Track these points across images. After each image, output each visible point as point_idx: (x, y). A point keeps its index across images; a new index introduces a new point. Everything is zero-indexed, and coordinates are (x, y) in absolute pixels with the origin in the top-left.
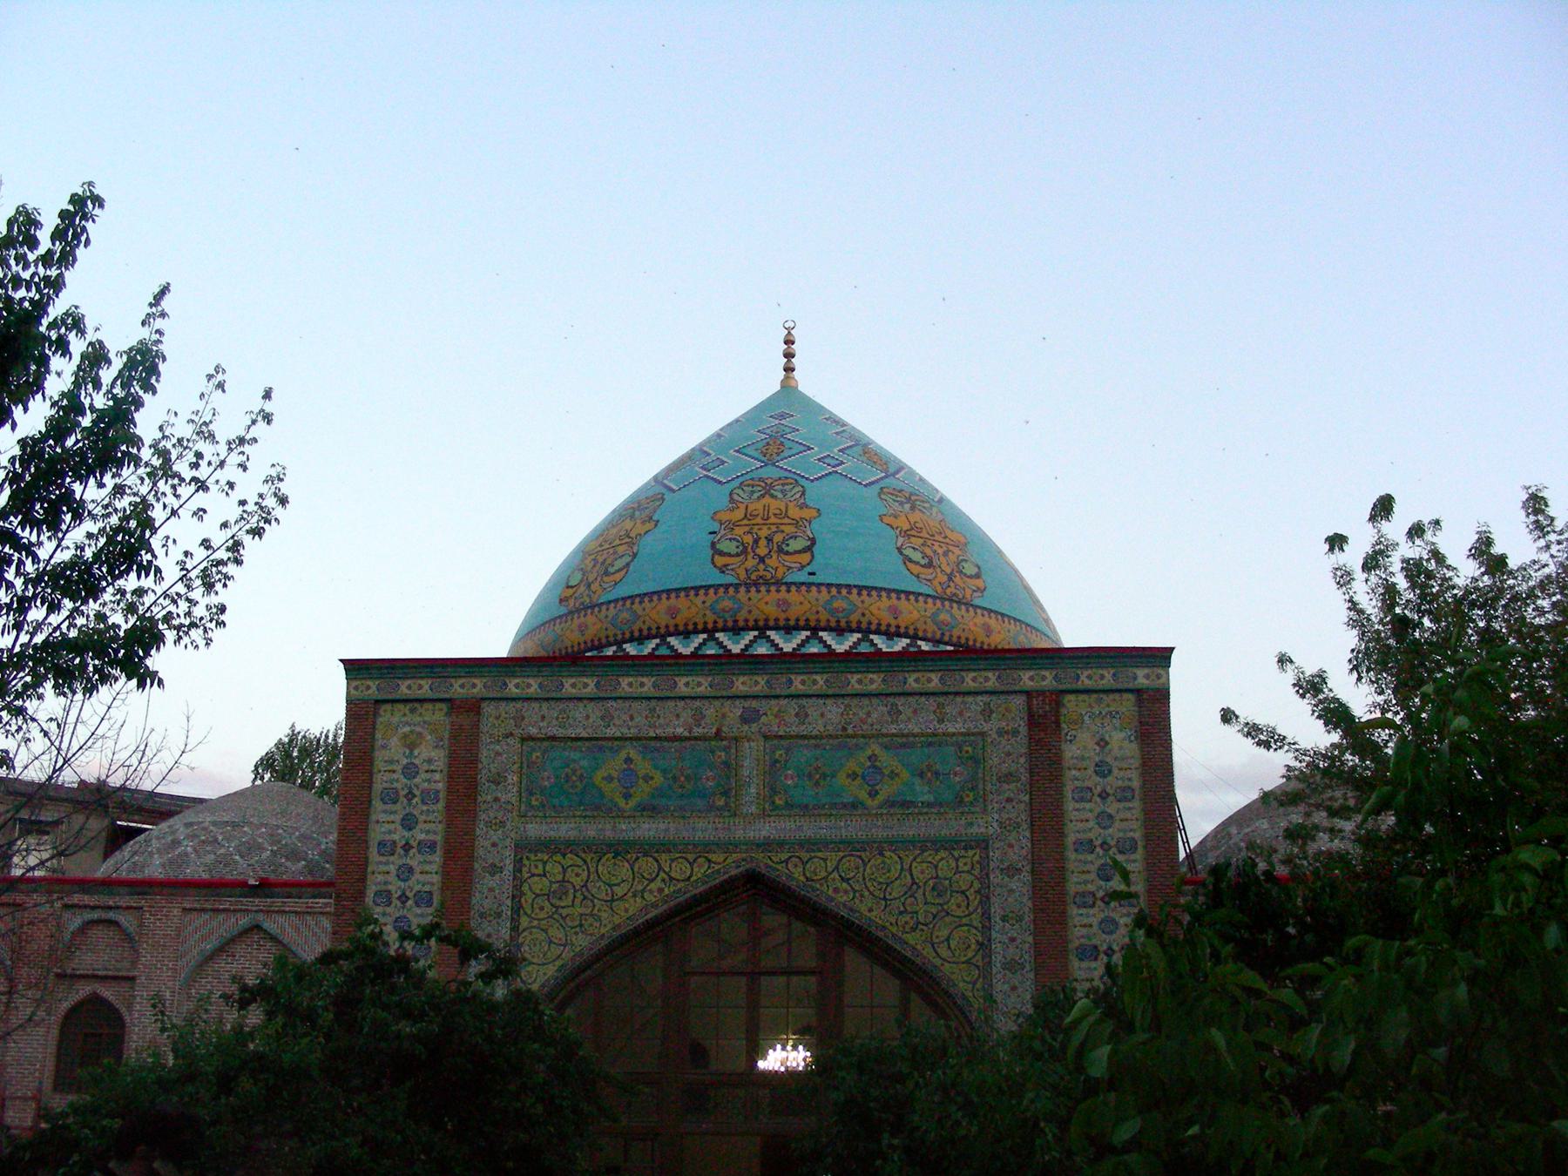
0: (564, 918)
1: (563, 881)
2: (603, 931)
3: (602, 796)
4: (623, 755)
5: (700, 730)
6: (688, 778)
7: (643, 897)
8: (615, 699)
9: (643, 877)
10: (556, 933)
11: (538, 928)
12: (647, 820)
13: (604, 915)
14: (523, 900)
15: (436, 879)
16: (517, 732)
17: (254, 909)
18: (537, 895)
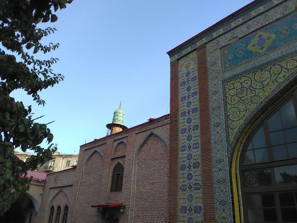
0: (244, 101)
1: (242, 87)
2: (261, 100)
3: (251, 52)
4: (258, 35)
5: (287, 12)
6: (287, 30)
7: (277, 81)
8: (250, 20)
9: (275, 74)
10: (242, 107)
11: (234, 107)
12: (272, 53)
13: (261, 94)
14: (227, 100)
15: (198, 103)
16: (218, 47)
17: (151, 128)
18: (233, 96)
